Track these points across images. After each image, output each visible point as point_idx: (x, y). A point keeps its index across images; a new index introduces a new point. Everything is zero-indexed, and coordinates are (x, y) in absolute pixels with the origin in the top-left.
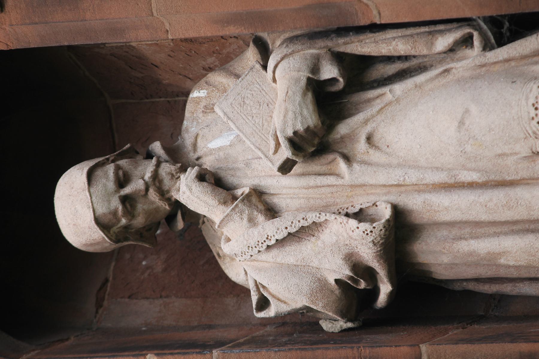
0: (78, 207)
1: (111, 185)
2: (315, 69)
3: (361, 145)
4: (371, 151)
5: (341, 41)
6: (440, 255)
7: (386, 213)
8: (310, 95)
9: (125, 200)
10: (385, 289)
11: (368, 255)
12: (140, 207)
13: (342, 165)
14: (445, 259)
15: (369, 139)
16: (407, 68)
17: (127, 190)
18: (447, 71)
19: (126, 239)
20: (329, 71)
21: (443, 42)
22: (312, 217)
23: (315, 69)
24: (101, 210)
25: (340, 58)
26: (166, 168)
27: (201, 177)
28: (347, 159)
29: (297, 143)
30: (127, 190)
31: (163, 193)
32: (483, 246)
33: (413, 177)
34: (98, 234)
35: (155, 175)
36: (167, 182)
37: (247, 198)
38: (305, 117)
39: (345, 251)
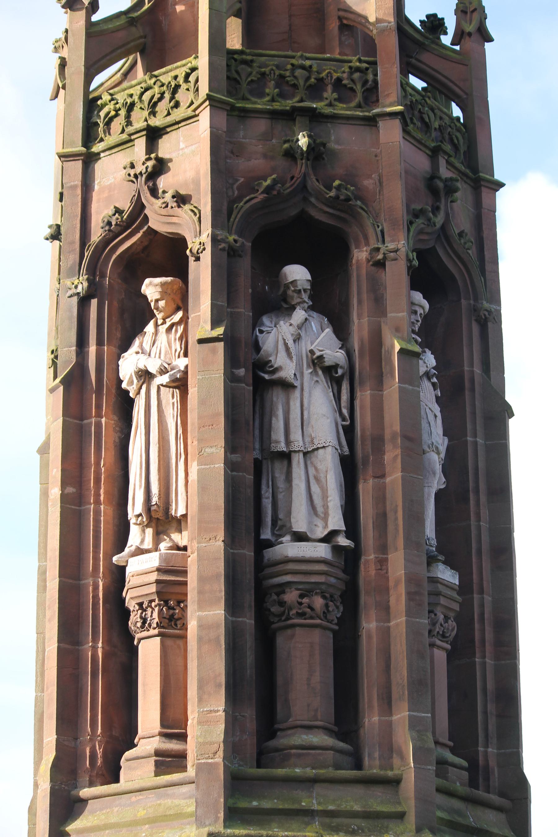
0: (297, 274)
1: (305, 287)
2: (341, 367)
3: (315, 379)
4: (314, 381)
5: (348, 377)
6: (277, 397)
7: (295, 384)
8: (334, 364)
9: (300, 291)
10: (267, 377)
11: (282, 374)
12: (295, 295)
13: (310, 371)
14: (275, 399)
15: (317, 381)
16: (338, 398)
17: (303, 292)
18: (336, 411)
19: (284, 287)
20: (340, 372)
21: (345, 412)
22: (294, 358)
23: (341, 367)
24: (299, 283)
25: (342, 376)
26: (306, 305)
27: (306, 319)
28: (311, 373)
29: (321, 357)
30: (303, 292)
31: (299, 303)
32: (280, 413)
33: (306, 394)
34: (290, 280)
35: (305, 302)
36: (302, 305)
37: (299, 334)
38: (328, 362)
39: (283, 367)
